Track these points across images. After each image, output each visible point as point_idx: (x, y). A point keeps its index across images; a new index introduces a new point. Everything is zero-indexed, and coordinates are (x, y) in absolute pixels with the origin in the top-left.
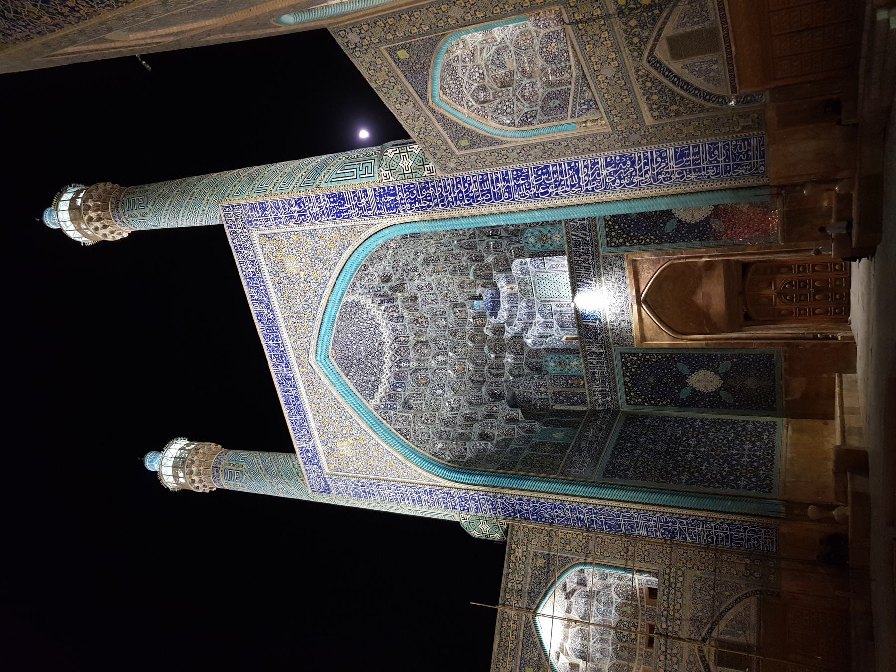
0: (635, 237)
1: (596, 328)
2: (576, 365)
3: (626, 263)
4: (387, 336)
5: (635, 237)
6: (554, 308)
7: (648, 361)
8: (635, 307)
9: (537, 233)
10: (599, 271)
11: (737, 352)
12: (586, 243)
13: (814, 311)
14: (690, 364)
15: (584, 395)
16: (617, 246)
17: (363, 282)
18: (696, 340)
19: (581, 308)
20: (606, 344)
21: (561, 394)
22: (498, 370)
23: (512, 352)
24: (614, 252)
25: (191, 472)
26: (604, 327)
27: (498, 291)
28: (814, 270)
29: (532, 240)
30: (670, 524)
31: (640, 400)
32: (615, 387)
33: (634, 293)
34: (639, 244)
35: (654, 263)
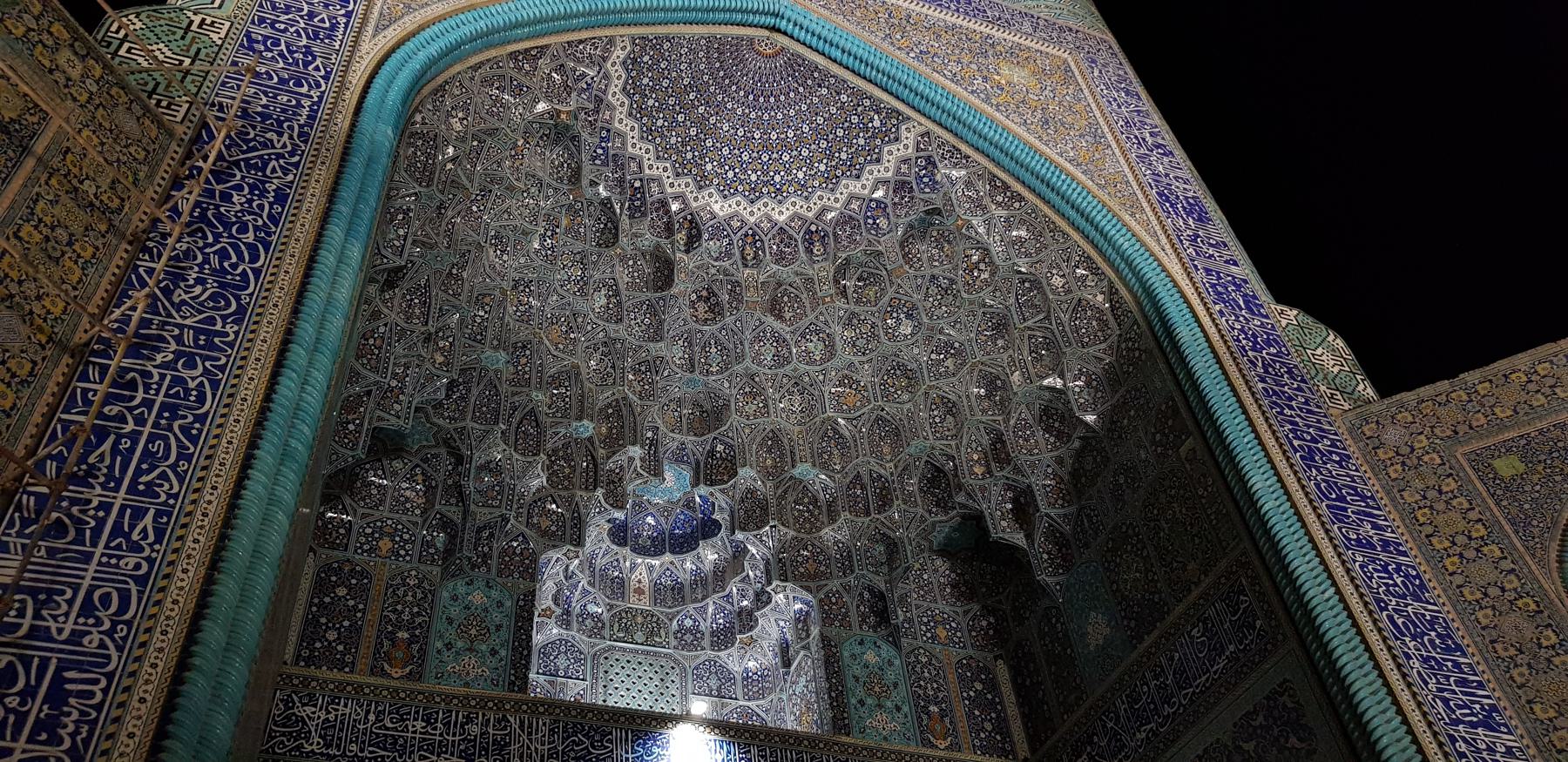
2: (467, 671)
9: (890, 676)
21: (361, 592)
22: (529, 433)
23: (540, 498)
29: (871, 657)
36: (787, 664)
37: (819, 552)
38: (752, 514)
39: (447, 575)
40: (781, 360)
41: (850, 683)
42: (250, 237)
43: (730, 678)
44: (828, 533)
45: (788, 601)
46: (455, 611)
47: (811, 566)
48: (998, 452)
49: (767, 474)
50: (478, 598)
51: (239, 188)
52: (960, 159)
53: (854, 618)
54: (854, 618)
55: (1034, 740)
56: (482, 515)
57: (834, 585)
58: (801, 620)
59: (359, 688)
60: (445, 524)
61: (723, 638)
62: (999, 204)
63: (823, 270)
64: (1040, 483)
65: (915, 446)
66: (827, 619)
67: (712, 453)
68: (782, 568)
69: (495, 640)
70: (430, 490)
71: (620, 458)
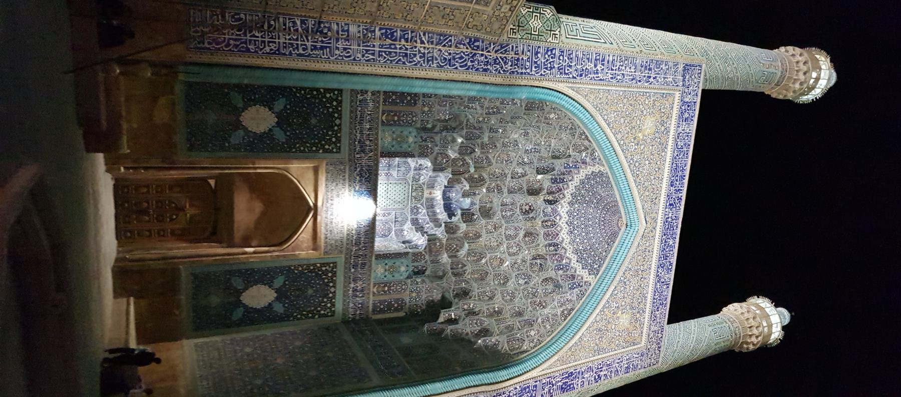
0: (311, 272)
1: (360, 181)
3: (323, 248)
4: (563, 208)
5: (311, 272)
6: (395, 173)
7: (313, 145)
8: (319, 204)
9: (396, 275)
10: (348, 239)
11: (223, 154)
12: (355, 266)
13: (148, 192)
14: (272, 139)
15: (385, 101)
16: (328, 264)
17: (569, 298)
18: (265, 167)
19: (371, 201)
20: (353, 162)
22: (465, 151)
23: (447, 156)
24: (330, 258)
25: (801, 84)
26: (352, 180)
27: (444, 193)
28: (150, 231)
30: (319, 45)
31: (328, 95)
32: (351, 112)
33: (319, 218)
34: (309, 265)
35: (297, 248)
36: (404, 242)
37: (438, 253)
38: (450, 229)
39: (417, 129)
40: (508, 237)
41: (393, 261)
42: (469, 64)
43: (402, 225)
44: (445, 256)
45: (421, 241)
46: (405, 133)
47: (435, 250)
48: (471, 313)
49: (466, 235)
50: (411, 140)
51: (486, 58)
52: (579, 298)
53: (416, 264)
54: (416, 264)
55: (379, 322)
56: (437, 138)
57: (427, 257)
58: (416, 246)
59: (378, 108)
60: (434, 127)
61: (415, 222)
62: (563, 312)
63: (542, 251)
64: (459, 326)
65: (475, 285)
66: (414, 254)
67: (473, 215)
68: (432, 239)
69: (396, 146)
70: (446, 121)
71: (465, 183)
